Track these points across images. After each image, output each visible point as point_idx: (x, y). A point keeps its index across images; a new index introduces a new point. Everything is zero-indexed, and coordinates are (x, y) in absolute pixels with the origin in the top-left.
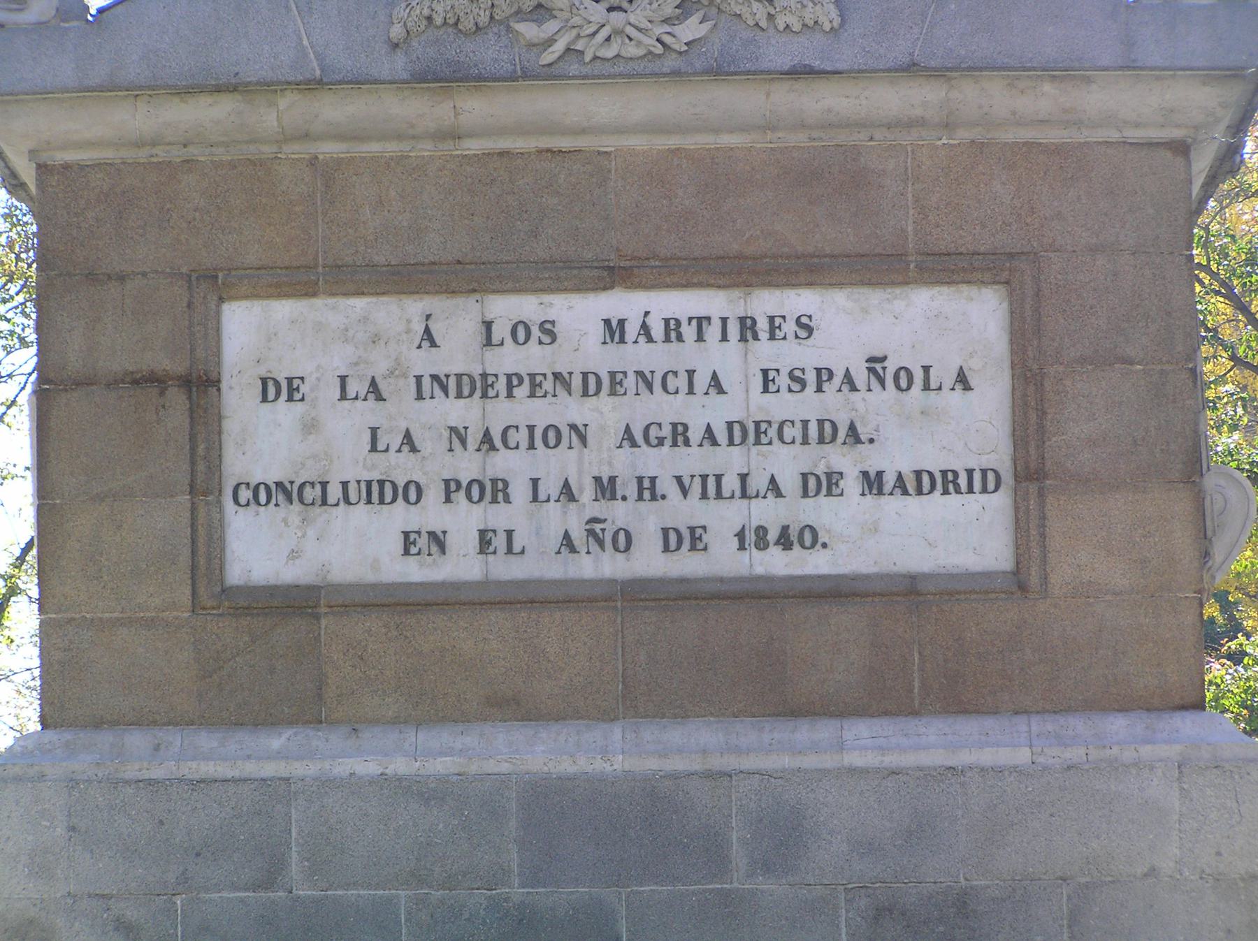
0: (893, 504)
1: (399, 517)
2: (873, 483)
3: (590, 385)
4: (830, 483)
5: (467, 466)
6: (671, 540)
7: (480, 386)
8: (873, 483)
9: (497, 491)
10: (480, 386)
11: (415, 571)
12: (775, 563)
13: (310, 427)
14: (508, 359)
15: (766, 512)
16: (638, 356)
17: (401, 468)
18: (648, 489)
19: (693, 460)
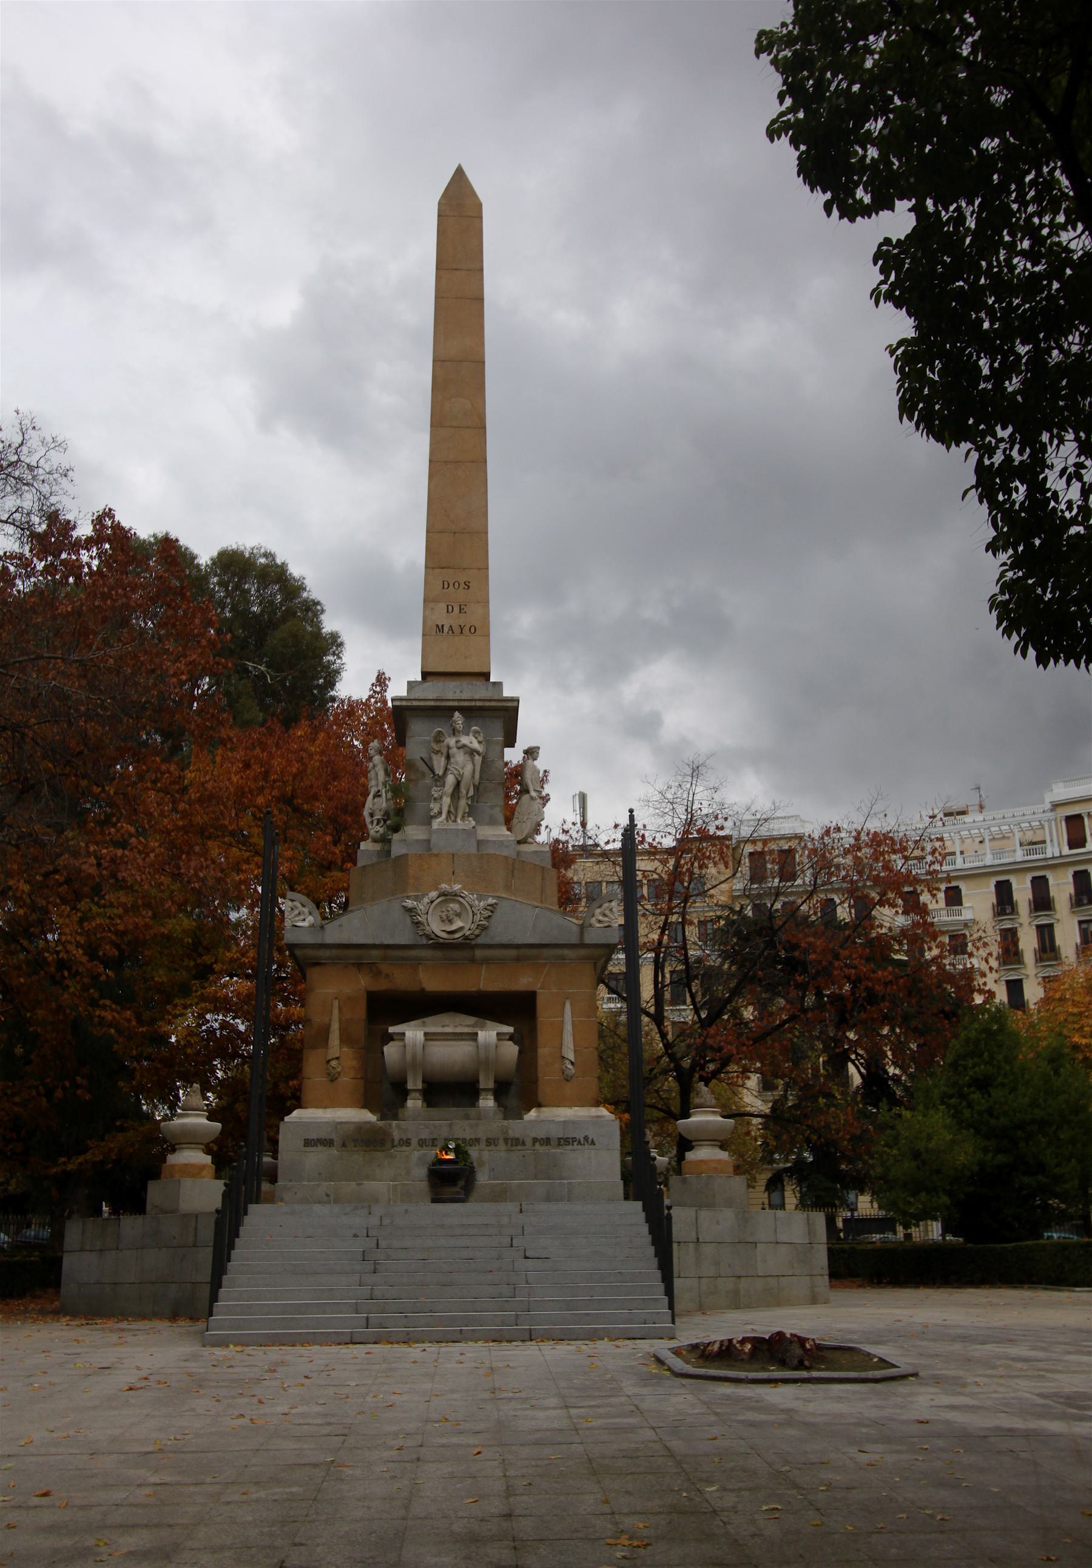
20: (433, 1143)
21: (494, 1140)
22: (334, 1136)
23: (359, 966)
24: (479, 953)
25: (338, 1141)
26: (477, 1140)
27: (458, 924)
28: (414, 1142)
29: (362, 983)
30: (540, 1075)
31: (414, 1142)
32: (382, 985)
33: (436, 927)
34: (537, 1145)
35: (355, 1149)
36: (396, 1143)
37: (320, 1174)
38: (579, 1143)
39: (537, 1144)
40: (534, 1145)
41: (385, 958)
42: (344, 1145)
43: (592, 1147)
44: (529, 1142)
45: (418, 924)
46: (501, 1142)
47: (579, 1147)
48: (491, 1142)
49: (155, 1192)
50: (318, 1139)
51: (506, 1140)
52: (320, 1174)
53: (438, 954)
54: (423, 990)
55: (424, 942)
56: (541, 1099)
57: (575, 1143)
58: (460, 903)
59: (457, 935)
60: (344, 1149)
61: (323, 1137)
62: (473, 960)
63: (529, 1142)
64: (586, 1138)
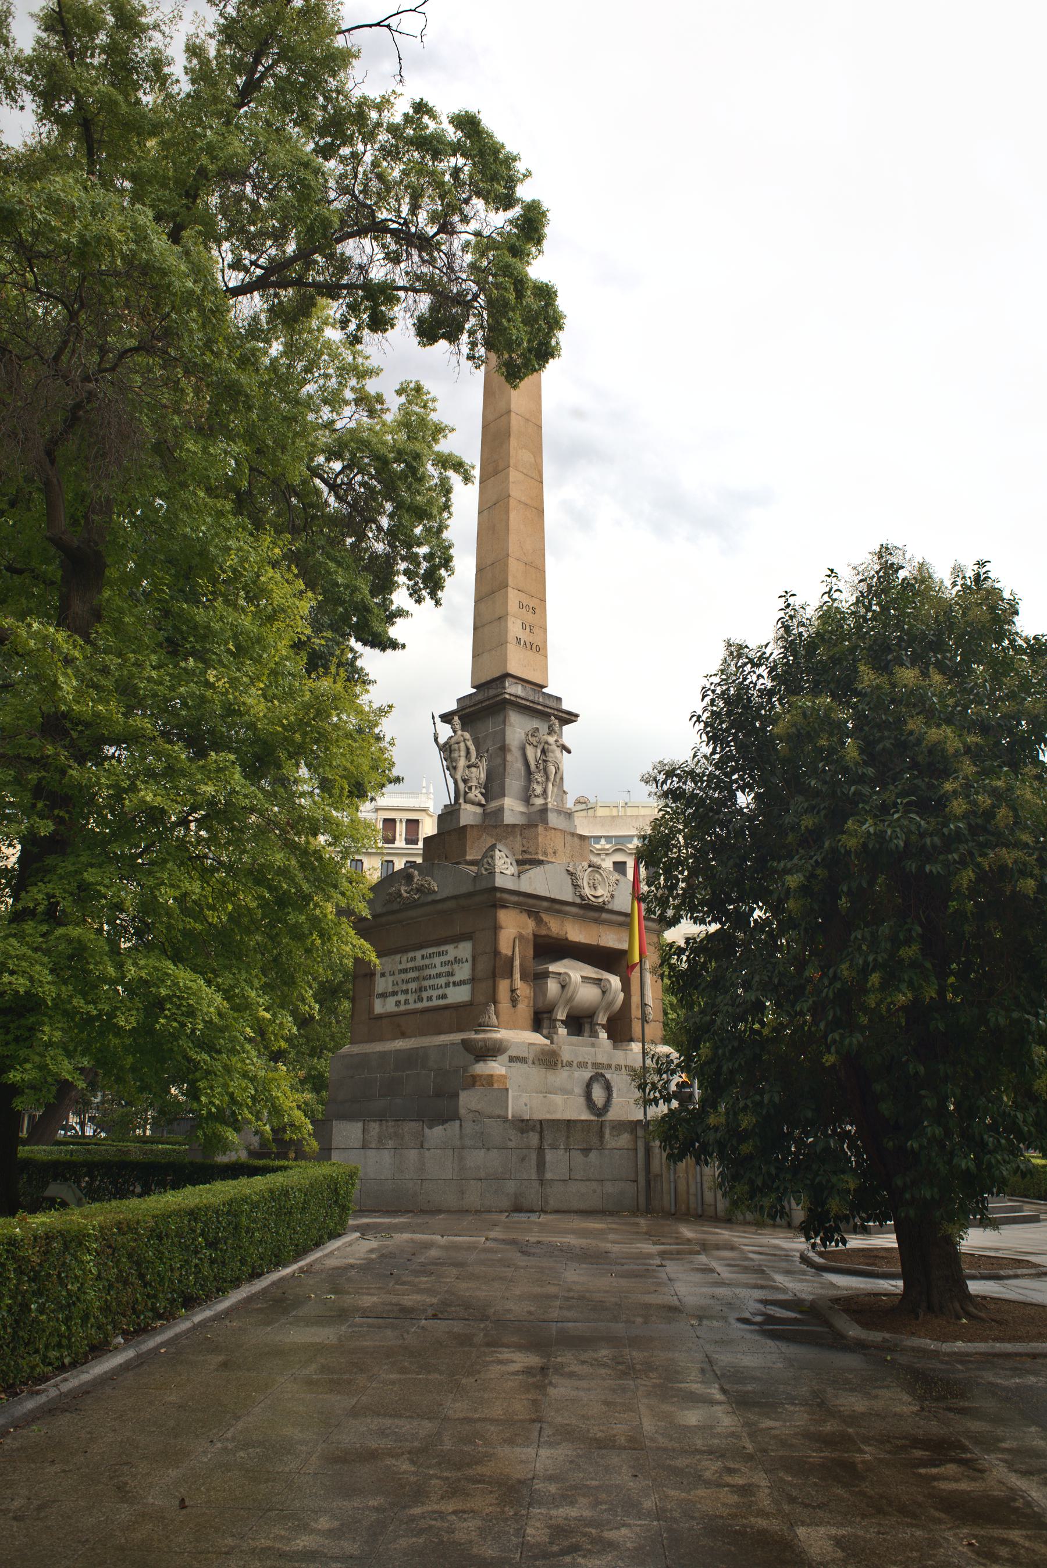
0: (457, 988)
1: (396, 998)
2: (454, 984)
3: (421, 968)
4: (447, 985)
5: (404, 987)
6: (430, 999)
7: (405, 971)
8: (454, 984)
9: (406, 992)
10: (405, 971)
11: (396, 1009)
12: (442, 1002)
13: (386, 981)
14: (410, 965)
15: (440, 992)
16: (427, 962)
17: (396, 989)
18: (426, 990)
19: (431, 982)
22: (525, 1055)
23: (530, 913)
24: (604, 916)
25: (530, 1061)
26: (610, 1066)
27: (599, 892)
28: (575, 1064)
29: (529, 926)
32: (544, 932)
33: (587, 891)
41: (547, 910)
42: (533, 1063)
45: (576, 886)
48: (618, 1068)
49: (468, 1100)
53: (581, 912)
54: (567, 939)
55: (578, 901)
58: (601, 874)
59: (600, 900)
62: (596, 921)
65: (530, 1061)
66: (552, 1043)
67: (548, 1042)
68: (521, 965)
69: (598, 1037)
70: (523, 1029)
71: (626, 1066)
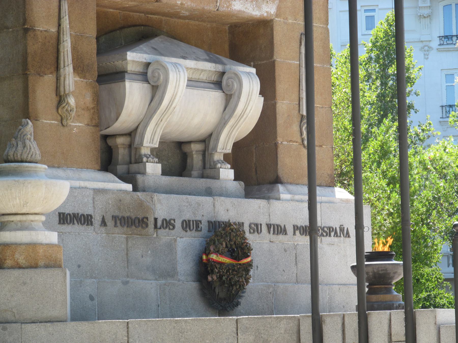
20: (197, 226)
21: (257, 225)
22: (88, 210)
25: (97, 220)
28: (178, 224)
30: (279, 140)
31: (178, 224)
34: (297, 232)
35: (117, 230)
36: (159, 223)
37: (79, 266)
38: (336, 235)
39: (297, 232)
40: (294, 234)
42: (104, 223)
43: (347, 239)
44: (290, 230)
46: (264, 229)
47: (336, 239)
50: (74, 214)
51: (269, 226)
52: (79, 266)
56: (282, 172)
57: (332, 234)
60: (103, 229)
61: (81, 212)
63: (290, 230)
64: (342, 229)
65: (97, 220)
66: (135, 189)
67: (129, 187)
68: (74, 49)
69: (216, 177)
70: (82, 167)
71: (269, 226)
